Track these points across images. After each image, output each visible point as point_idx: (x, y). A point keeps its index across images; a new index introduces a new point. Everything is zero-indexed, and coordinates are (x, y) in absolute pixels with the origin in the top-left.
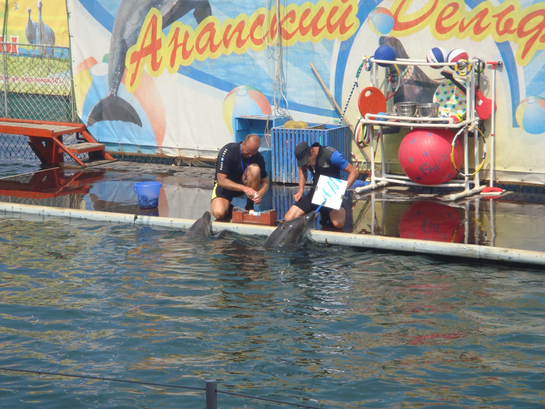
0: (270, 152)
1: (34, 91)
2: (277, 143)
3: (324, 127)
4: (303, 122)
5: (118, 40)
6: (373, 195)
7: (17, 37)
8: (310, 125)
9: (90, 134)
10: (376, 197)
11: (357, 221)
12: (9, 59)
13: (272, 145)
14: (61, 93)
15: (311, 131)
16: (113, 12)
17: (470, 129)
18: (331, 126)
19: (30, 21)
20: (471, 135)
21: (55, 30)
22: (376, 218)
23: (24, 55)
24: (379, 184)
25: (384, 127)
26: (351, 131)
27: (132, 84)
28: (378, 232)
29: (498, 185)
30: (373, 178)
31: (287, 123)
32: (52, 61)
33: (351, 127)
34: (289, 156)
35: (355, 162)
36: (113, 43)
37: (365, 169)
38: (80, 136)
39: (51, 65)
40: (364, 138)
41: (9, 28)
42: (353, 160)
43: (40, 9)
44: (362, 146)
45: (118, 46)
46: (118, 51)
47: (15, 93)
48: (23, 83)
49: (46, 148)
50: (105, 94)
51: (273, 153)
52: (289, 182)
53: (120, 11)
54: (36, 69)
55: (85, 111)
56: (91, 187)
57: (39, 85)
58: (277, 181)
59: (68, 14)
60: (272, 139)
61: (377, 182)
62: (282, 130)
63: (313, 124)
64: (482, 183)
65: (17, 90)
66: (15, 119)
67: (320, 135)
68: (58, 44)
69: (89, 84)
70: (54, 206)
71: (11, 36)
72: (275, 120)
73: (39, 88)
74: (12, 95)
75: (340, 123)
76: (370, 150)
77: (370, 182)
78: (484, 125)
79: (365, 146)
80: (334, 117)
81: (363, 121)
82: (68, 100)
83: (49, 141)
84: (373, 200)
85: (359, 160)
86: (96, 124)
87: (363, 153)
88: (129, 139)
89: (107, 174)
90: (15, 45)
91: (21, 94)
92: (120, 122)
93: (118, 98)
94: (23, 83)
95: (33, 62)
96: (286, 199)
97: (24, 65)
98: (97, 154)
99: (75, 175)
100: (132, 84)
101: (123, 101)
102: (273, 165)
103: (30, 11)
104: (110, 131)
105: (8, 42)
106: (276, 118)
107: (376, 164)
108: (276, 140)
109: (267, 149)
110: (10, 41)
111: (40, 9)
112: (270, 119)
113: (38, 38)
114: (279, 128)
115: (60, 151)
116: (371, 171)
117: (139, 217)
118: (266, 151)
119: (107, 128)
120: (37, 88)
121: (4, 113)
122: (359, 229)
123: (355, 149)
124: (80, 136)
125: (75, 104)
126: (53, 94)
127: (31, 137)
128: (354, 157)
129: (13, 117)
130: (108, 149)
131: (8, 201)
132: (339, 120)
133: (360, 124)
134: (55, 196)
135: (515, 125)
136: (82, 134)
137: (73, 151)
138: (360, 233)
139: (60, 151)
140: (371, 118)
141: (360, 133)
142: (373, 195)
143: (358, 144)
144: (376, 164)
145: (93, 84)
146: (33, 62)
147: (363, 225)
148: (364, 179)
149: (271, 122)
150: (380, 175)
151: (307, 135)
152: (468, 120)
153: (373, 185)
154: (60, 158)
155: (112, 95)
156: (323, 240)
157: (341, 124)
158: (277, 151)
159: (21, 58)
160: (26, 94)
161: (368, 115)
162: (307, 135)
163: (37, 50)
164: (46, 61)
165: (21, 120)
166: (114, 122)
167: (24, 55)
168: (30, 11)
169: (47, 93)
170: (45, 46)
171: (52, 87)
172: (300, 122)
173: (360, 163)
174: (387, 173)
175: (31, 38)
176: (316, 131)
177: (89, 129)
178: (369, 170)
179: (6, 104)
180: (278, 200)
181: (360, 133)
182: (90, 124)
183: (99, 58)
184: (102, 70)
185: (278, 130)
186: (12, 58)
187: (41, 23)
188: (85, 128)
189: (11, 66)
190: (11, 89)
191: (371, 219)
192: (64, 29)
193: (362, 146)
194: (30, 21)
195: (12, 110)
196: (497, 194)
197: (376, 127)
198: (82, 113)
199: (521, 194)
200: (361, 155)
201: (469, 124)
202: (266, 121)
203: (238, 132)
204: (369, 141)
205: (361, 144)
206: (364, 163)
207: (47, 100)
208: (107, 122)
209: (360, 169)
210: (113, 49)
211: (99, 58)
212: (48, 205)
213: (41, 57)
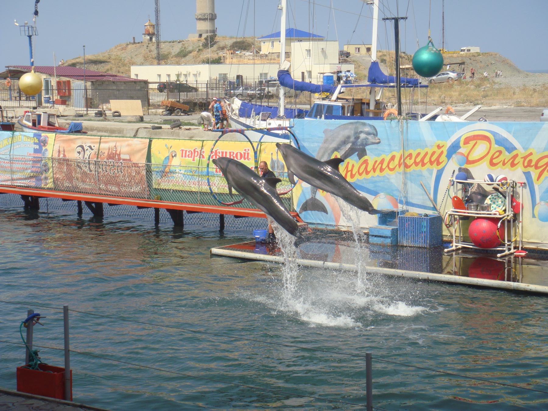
0: (397, 229)
3: (426, 215)
8: (419, 214)
10: (456, 254)
11: (445, 268)
17: (509, 218)
18: (431, 215)
19: (272, 159)
20: (509, 221)
28: (456, 273)
29: (523, 249)
30: (454, 244)
31: (407, 213)
44: (448, 226)
50: (309, 196)
53: (318, 153)
55: (298, 206)
61: (456, 246)
64: (515, 248)
69: (301, 192)
76: (452, 230)
78: (516, 217)
79: (450, 226)
84: (454, 256)
86: (304, 213)
87: (449, 230)
88: (320, 220)
92: (316, 212)
93: (315, 199)
103: (272, 154)
109: (396, 227)
113: (276, 168)
119: (309, 215)
122: (446, 271)
123: (444, 227)
125: (293, 202)
132: (436, 212)
135: (534, 216)
141: (447, 219)
142: (454, 253)
143: (446, 225)
145: (303, 191)
147: (448, 269)
149: (398, 212)
152: (507, 213)
153: (454, 248)
155: (312, 197)
156: (426, 277)
166: (313, 212)
168: (272, 154)
177: (300, 215)
182: (300, 213)
188: (298, 215)
191: (453, 267)
194: (272, 159)
196: (523, 254)
197: (456, 216)
198: (296, 207)
199: (536, 255)
201: (508, 216)
204: (452, 224)
208: (309, 212)
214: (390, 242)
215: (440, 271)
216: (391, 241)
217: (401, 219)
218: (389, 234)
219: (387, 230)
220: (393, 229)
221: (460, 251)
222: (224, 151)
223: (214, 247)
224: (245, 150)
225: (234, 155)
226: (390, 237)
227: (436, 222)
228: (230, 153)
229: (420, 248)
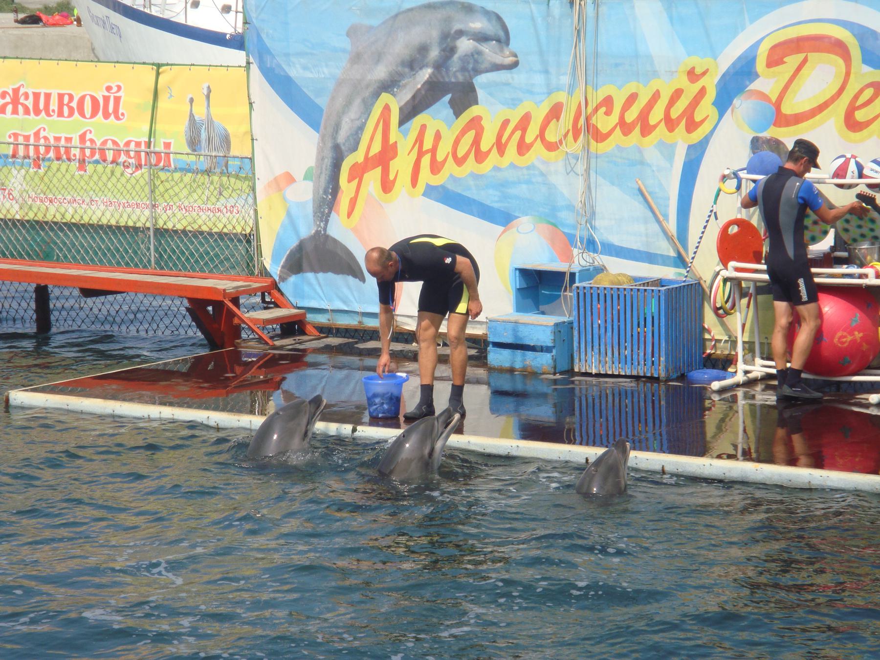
0: (571, 323)
1: (196, 227)
2: (582, 310)
3: (660, 282)
4: (624, 275)
5: (329, 144)
6: (740, 393)
7: (172, 141)
8: (635, 279)
9: (282, 294)
11: (714, 437)
12: (158, 177)
13: (575, 313)
14: (239, 229)
15: (638, 290)
16: (322, 101)
18: (671, 282)
19: (192, 115)
21: (230, 129)
22: (745, 431)
23: (182, 170)
24: (750, 375)
25: (759, 284)
26: (703, 289)
27: (349, 215)
28: (747, 456)
30: (741, 366)
31: (599, 276)
32: (225, 179)
33: (702, 282)
34: (602, 330)
35: (711, 340)
36: (320, 150)
37: (727, 352)
38: (268, 299)
39: (222, 185)
40: (727, 302)
41: (159, 127)
42: (707, 336)
43: (208, 97)
44: (721, 313)
45: (329, 155)
46: (328, 162)
47: (167, 230)
48: (179, 215)
49: (213, 317)
50: (306, 229)
51: (575, 325)
52: (602, 372)
53: (333, 98)
54: (199, 191)
55: (275, 258)
56: (284, 379)
57: (204, 217)
58: (583, 371)
59: (251, 104)
60: (575, 302)
61: (746, 372)
62: (591, 288)
63: (641, 279)
65: (170, 226)
66: (166, 271)
67: (653, 297)
68: (234, 152)
69: (283, 215)
70: (223, 410)
71: (162, 141)
72: (580, 272)
73: (205, 222)
74: (161, 233)
75: (686, 277)
76: (736, 321)
77: (736, 372)
79: (727, 313)
80: (677, 266)
81: (725, 273)
82: (249, 239)
83: (219, 305)
84: (741, 402)
85: (717, 337)
86: (293, 279)
87: (723, 324)
88: (344, 302)
89: (309, 358)
90: (168, 155)
91: (176, 232)
92: (330, 275)
93: (327, 237)
94: (179, 215)
95: (194, 181)
96: (597, 401)
97: (182, 185)
98: (293, 327)
99: (258, 361)
100: (349, 215)
101: (335, 241)
102: (576, 344)
104: (315, 290)
105: (157, 149)
106: (580, 268)
107: (744, 342)
108: (581, 304)
109: (566, 319)
110: (160, 148)
111: (208, 97)
112: (572, 271)
113: (204, 143)
114: (585, 284)
115: (236, 321)
116: (737, 355)
117: (359, 428)
118: (564, 322)
119: (310, 284)
120: (200, 222)
121: (149, 261)
123: (710, 319)
124: (268, 299)
125: (259, 247)
126: (225, 230)
127: (190, 300)
128: (709, 332)
129: (162, 268)
130: (310, 317)
131: (154, 403)
133: (719, 278)
134: (227, 394)
136: (271, 294)
137: (255, 321)
138: (719, 457)
139: (236, 321)
140: (737, 269)
142: (740, 393)
143: (716, 310)
144: (744, 342)
145: (289, 214)
146: (194, 181)
148: (725, 369)
149: (573, 275)
150: (752, 362)
151: (632, 296)
153: (740, 378)
154: (236, 331)
156: (658, 468)
157: (688, 279)
158: (582, 322)
159: (177, 175)
160: (184, 231)
161: (732, 264)
162: (632, 296)
163: (203, 163)
164: (216, 178)
165: (175, 272)
166: (321, 275)
167: (182, 170)
169: (215, 230)
170: (215, 155)
171: (224, 220)
172: (619, 275)
173: (719, 341)
174: (763, 358)
175: (194, 143)
176: (645, 290)
177: (282, 286)
178: (733, 353)
179: (152, 247)
180: (584, 402)
181: (720, 294)
182: (283, 279)
183: (299, 175)
184: (304, 193)
185: (584, 288)
186: (163, 175)
187: (210, 121)
188: (275, 286)
189: (161, 189)
190: (161, 223)
191: (737, 434)
192: (245, 128)
193: (721, 313)
194: (192, 115)
195: (161, 256)
200: (720, 328)
202: (563, 274)
203: (520, 290)
205: (721, 312)
206: (726, 341)
207: (216, 240)
208: (310, 276)
209: (719, 352)
210: (321, 159)
211: (299, 175)
212: (216, 409)
213: (208, 172)
214: (550, 361)
215: (701, 449)
216: (555, 361)
217: (583, 296)
218: (545, 338)
219: (540, 326)
220: (557, 325)
221: (759, 388)
222: (43, 91)
223: (15, 387)
224: (109, 89)
225: (74, 105)
226: (548, 350)
227: (686, 299)
228: (61, 96)
229: (637, 378)
